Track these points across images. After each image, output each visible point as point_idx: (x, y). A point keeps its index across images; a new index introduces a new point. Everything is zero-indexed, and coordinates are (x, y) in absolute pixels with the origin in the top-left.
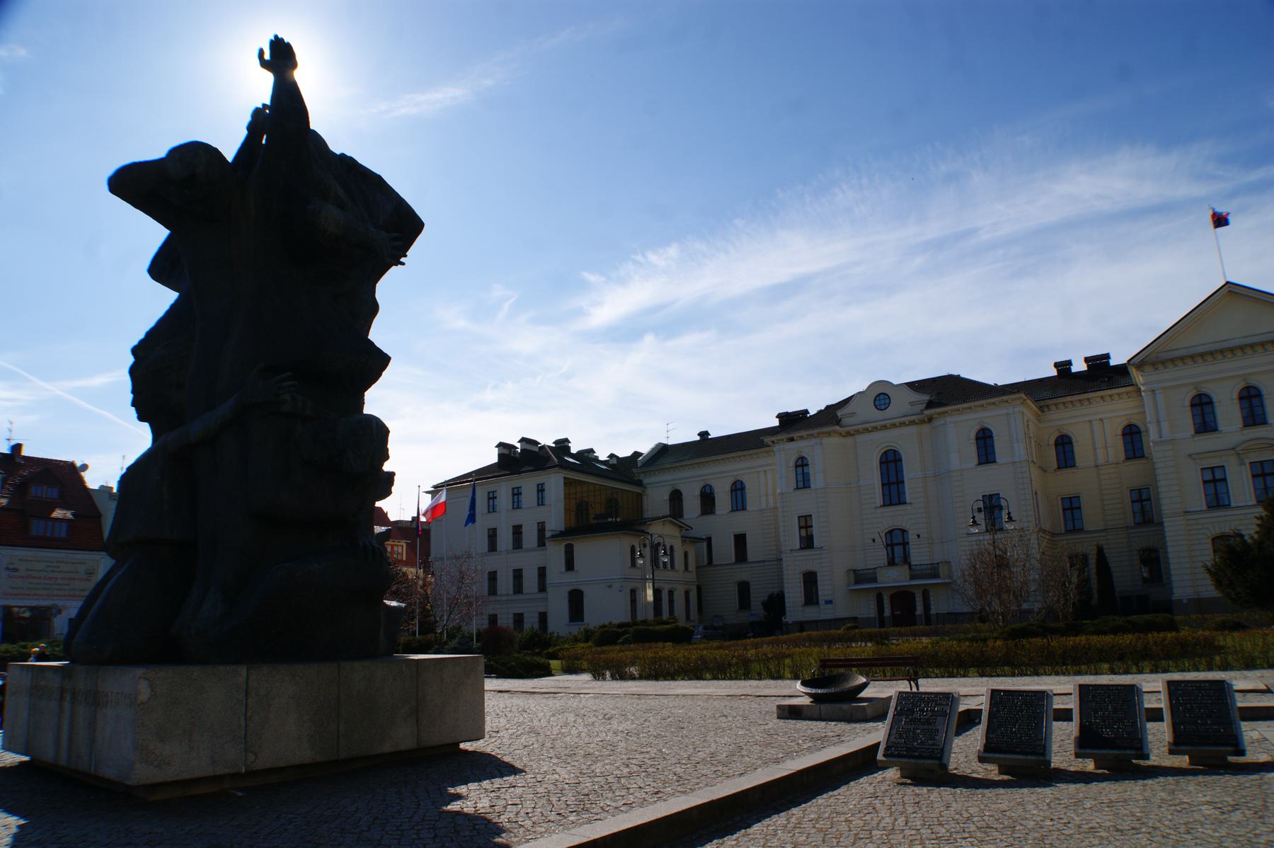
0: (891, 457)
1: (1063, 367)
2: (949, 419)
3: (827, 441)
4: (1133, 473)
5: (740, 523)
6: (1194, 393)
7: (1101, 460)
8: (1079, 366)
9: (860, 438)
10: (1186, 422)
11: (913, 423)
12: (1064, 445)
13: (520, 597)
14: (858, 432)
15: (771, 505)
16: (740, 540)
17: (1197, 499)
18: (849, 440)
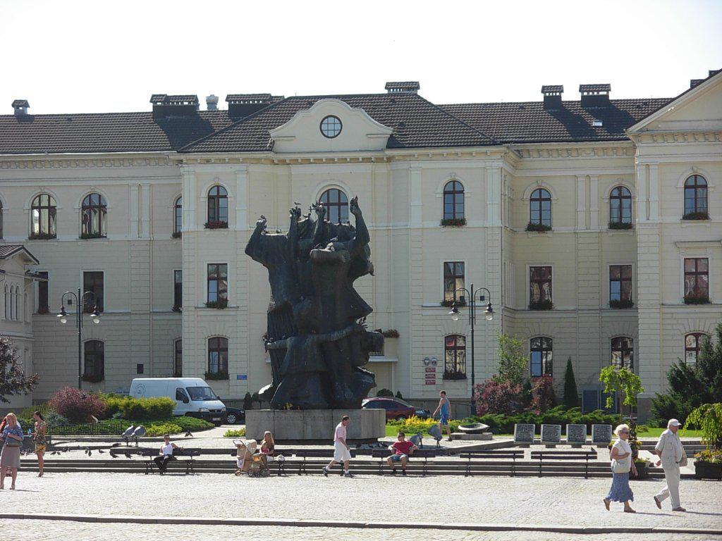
0: (334, 199)
1: (552, 95)
2: (414, 164)
3: (255, 168)
4: (613, 248)
5: (93, 256)
6: (690, 173)
7: (581, 227)
8: (571, 95)
9: (296, 169)
10: (677, 204)
11: (368, 160)
12: (541, 198)
13: (248, 376)
14: (295, 161)
15: (146, 235)
16: (94, 282)
17: (677, 291)
18: (282, 170)
